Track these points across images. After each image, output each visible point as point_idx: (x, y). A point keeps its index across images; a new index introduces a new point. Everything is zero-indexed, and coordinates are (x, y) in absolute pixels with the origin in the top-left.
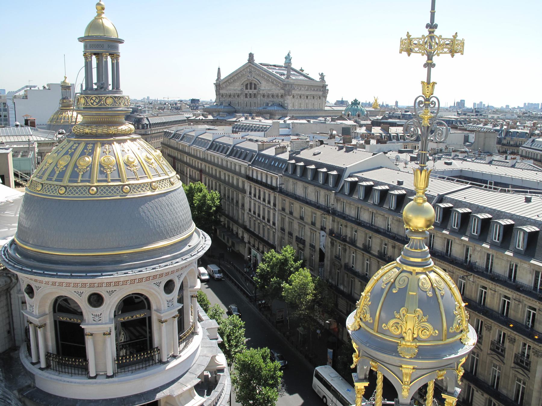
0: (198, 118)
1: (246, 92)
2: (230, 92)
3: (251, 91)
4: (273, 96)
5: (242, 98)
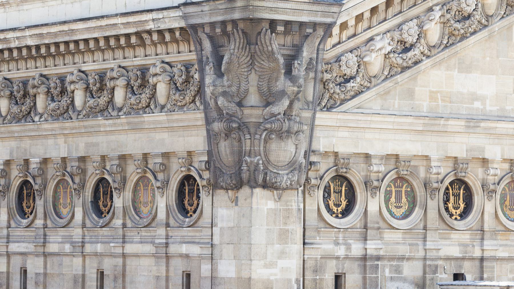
2: (460, 146)
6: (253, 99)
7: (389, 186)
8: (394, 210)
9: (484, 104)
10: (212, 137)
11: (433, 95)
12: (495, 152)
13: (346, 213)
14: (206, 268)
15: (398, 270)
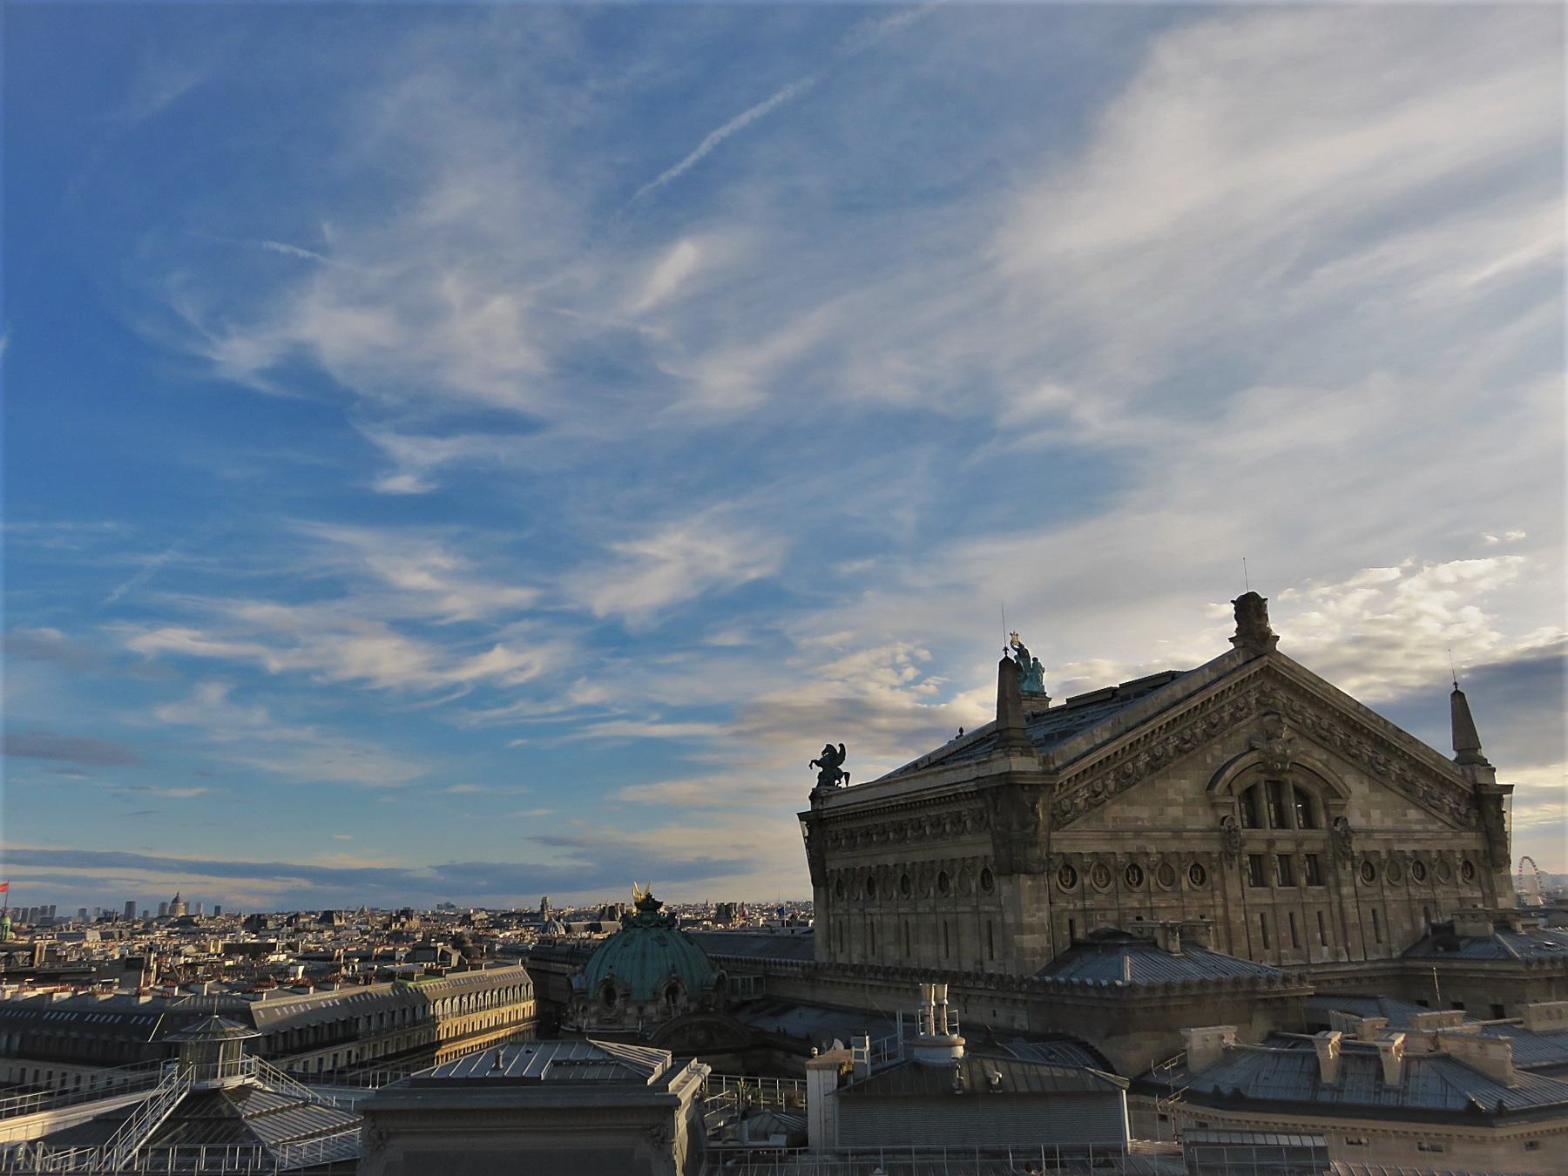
1: (1255, 840)
2: (1132, 846)
4: (1421, 869)
5: (1234, 891)
6: (1015, 827)
10: (995, 848)
11: (1114, 819)
12: (1152, 848)
13: (1072, 885)
14: (998, 918)
15: (1104, 916)
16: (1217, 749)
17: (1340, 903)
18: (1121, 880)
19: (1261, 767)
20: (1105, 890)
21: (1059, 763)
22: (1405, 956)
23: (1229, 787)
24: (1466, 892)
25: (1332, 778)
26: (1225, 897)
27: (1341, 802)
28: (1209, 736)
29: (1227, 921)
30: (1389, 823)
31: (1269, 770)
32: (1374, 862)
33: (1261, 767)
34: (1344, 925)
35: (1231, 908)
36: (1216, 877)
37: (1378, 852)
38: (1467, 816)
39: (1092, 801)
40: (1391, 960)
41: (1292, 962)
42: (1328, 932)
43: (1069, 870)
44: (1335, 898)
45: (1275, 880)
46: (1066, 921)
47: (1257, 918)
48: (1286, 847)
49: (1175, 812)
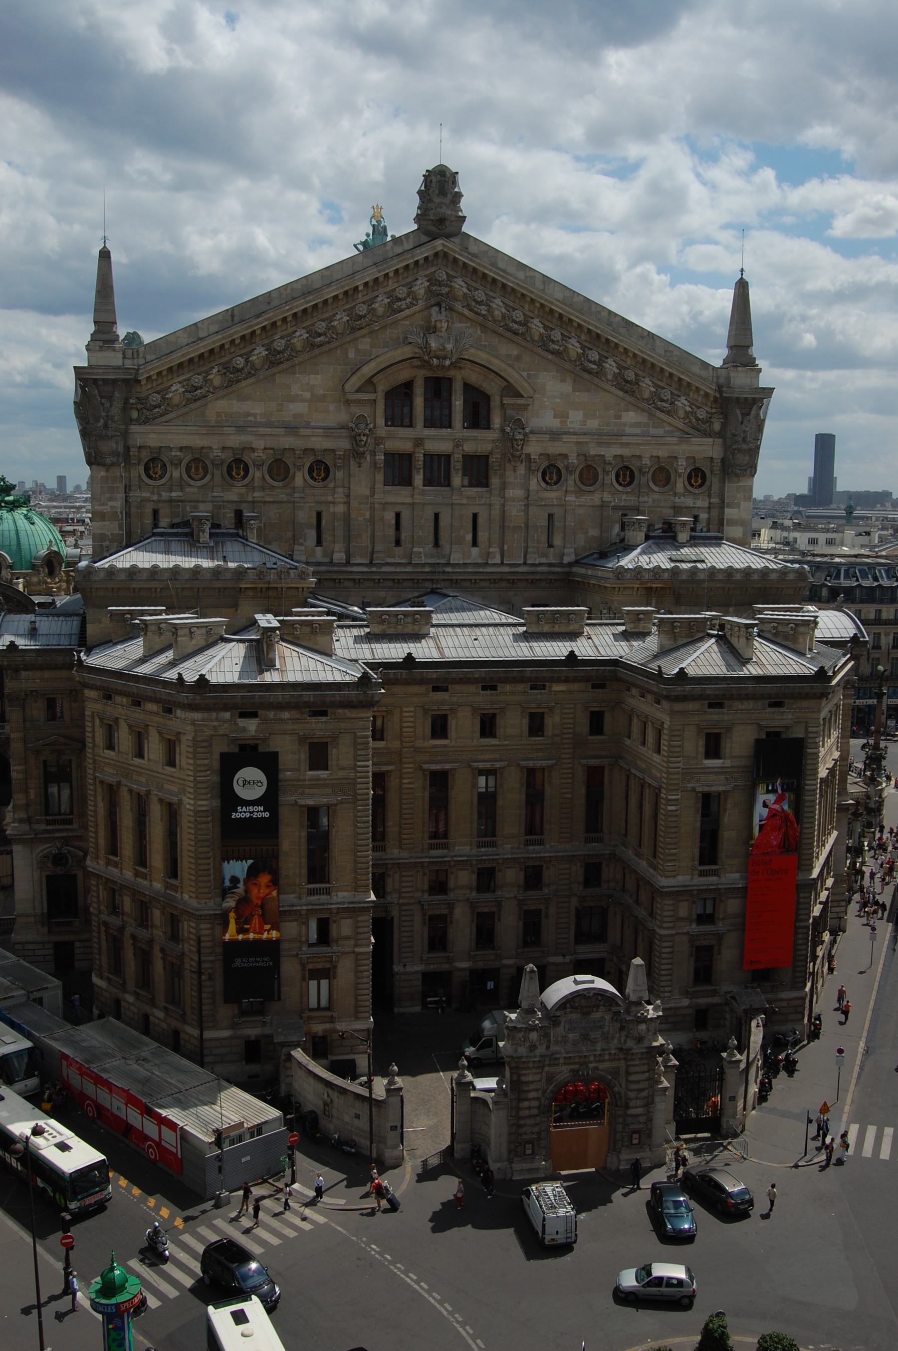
0: (190, 671)
1: (400, 440)
2: (235, 440)
3: (438, 442)
4: (626, 474)
5: (360, 488)
7: (189, 462)
8: (194, 476)
9: (256, 418)
11: (218, 415)
12: (260, 444)
13: (161, 477)
16: (365, 344)
17: (504, 505)
18: (217, 473)
19: (416, 362)
20: (199, 483)
21: (149, 358)
22: (577, 562)
23: (370, 384)
24: (689, 501)
25: (513, 376)
26: (348, 496)
27: (520, 401)
28: (353, 330)
29: (347, 519)
30: (593, 424)
31: (426, 365)
32: (561, 465)
33: (416, 362)
34: (503, 528)
35: (354, 504)
36: (340, 475)
37: (565, 456)
38: (708, 421)
39: (189, 395)
40: (561, 565)
41: (423, 560)
42: (482, 535)
43: (155, 464)
44: (496, 501)
45: (418, 479)
46: (148, 511)
47: (390, 517)
48: (443, 447)
49: (299, 408)
